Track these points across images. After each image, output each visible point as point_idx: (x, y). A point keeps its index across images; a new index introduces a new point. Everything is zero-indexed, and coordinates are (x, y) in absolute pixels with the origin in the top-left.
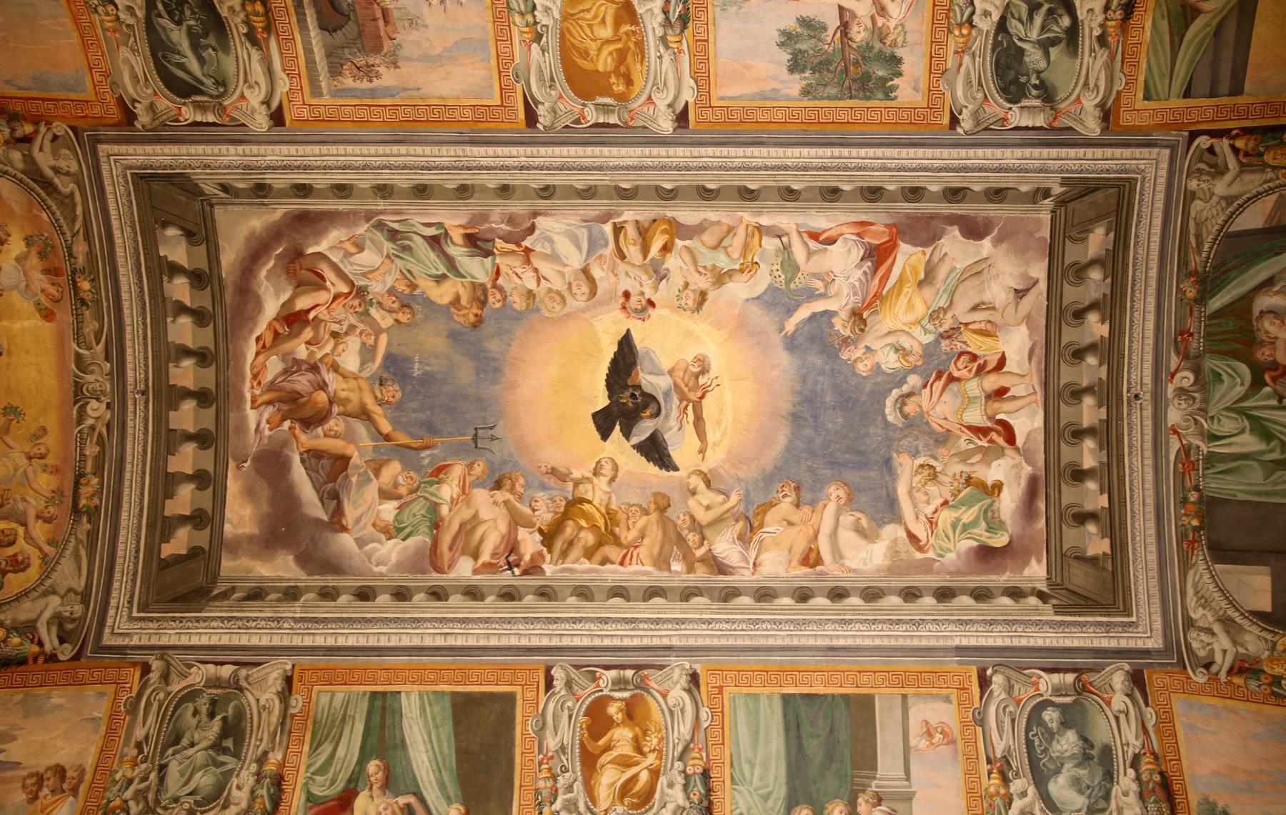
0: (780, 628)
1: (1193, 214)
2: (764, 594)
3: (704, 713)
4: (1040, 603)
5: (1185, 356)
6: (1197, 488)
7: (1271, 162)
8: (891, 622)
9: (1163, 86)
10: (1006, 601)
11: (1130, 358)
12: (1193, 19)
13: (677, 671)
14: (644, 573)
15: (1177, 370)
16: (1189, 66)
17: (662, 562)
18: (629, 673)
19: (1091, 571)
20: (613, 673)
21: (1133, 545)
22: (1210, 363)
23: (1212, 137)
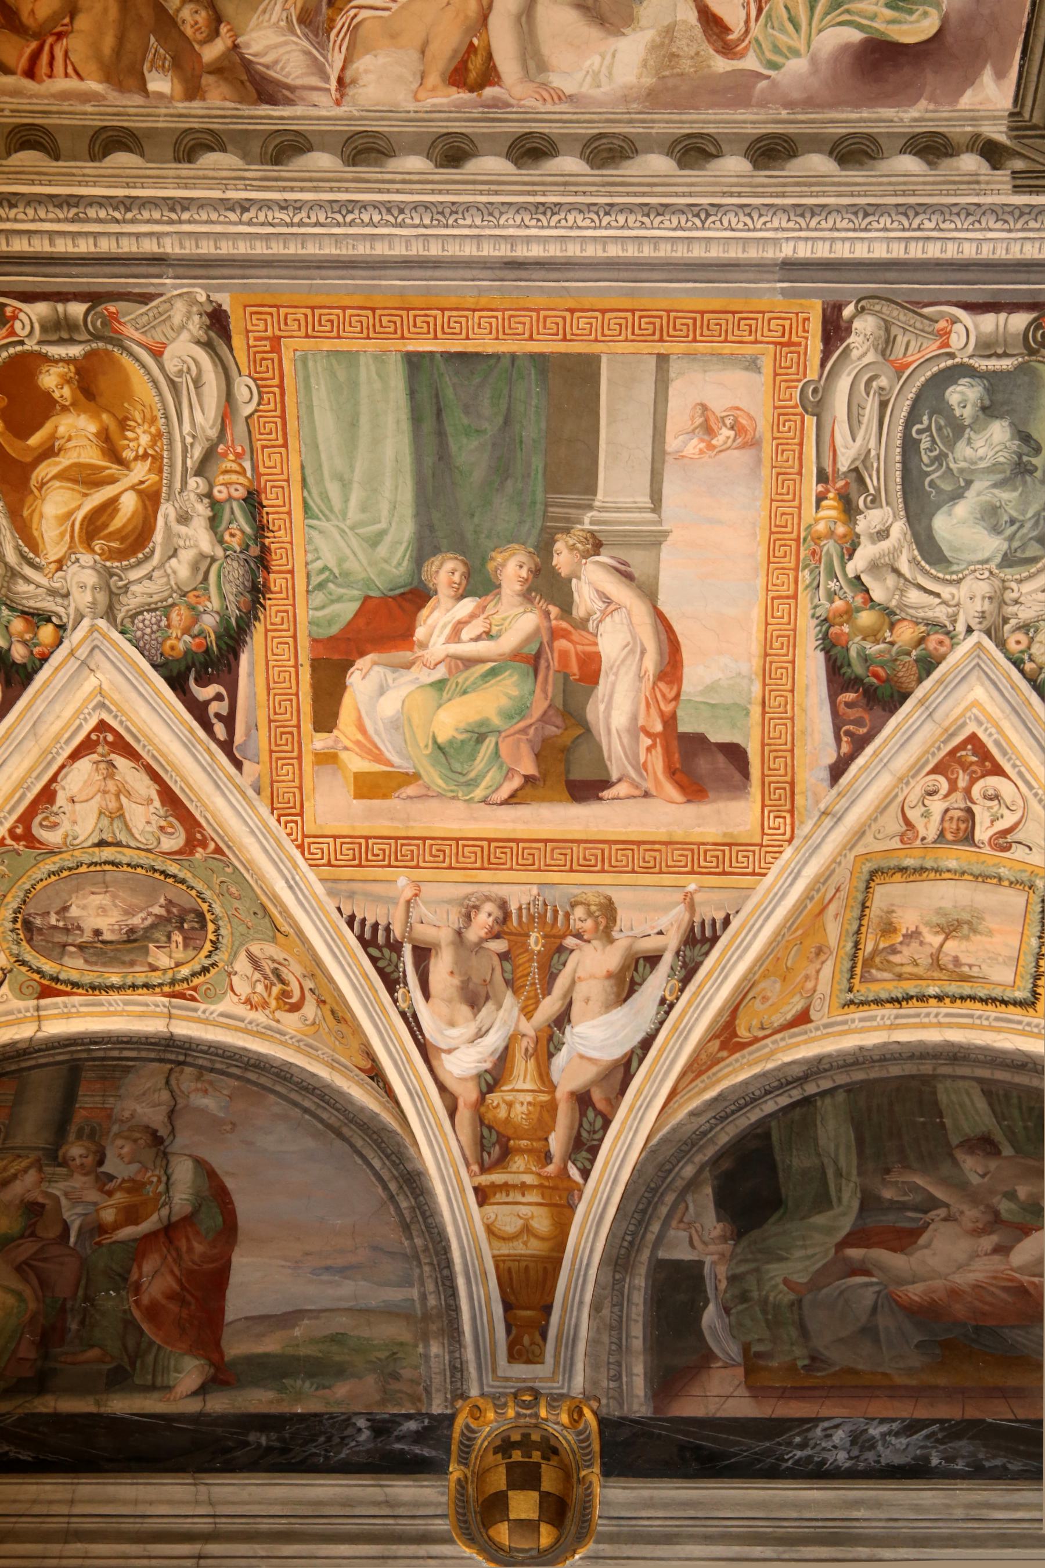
0: (400, 220)
2: (365, 148)
3: (243, 387)
4: (984, 167)
8: (646, 210)
10: (910, 164)
13: (180, 306)
14: (86, 97)
17: (124, 72)
18: (77, 309)
20: (41, 309)
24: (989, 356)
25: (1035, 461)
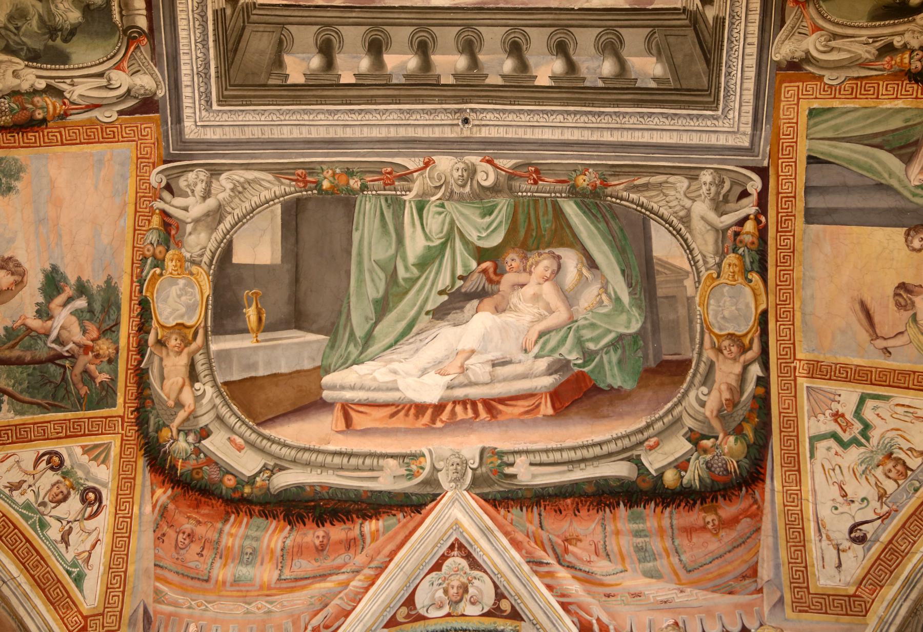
1: (672, 179)
5: (511, 176)
6: (364, 187)
7: (726, 261)
9: (825, 130)
11: (511, 111)
12: (900, 157)
15: (496, 166)
16: (844, 159)
19: (267, 59)
21: (298, 111)
22: (503, 204)
23: (759, 194)
24: (120, 6)
25: (59, 41)
